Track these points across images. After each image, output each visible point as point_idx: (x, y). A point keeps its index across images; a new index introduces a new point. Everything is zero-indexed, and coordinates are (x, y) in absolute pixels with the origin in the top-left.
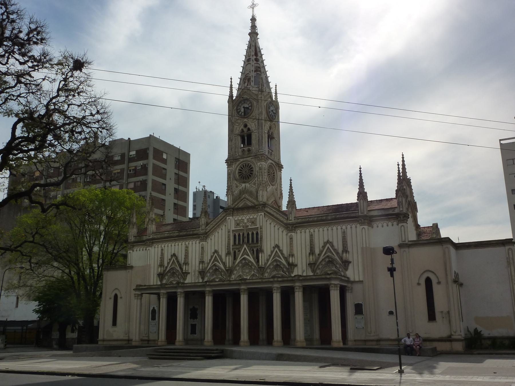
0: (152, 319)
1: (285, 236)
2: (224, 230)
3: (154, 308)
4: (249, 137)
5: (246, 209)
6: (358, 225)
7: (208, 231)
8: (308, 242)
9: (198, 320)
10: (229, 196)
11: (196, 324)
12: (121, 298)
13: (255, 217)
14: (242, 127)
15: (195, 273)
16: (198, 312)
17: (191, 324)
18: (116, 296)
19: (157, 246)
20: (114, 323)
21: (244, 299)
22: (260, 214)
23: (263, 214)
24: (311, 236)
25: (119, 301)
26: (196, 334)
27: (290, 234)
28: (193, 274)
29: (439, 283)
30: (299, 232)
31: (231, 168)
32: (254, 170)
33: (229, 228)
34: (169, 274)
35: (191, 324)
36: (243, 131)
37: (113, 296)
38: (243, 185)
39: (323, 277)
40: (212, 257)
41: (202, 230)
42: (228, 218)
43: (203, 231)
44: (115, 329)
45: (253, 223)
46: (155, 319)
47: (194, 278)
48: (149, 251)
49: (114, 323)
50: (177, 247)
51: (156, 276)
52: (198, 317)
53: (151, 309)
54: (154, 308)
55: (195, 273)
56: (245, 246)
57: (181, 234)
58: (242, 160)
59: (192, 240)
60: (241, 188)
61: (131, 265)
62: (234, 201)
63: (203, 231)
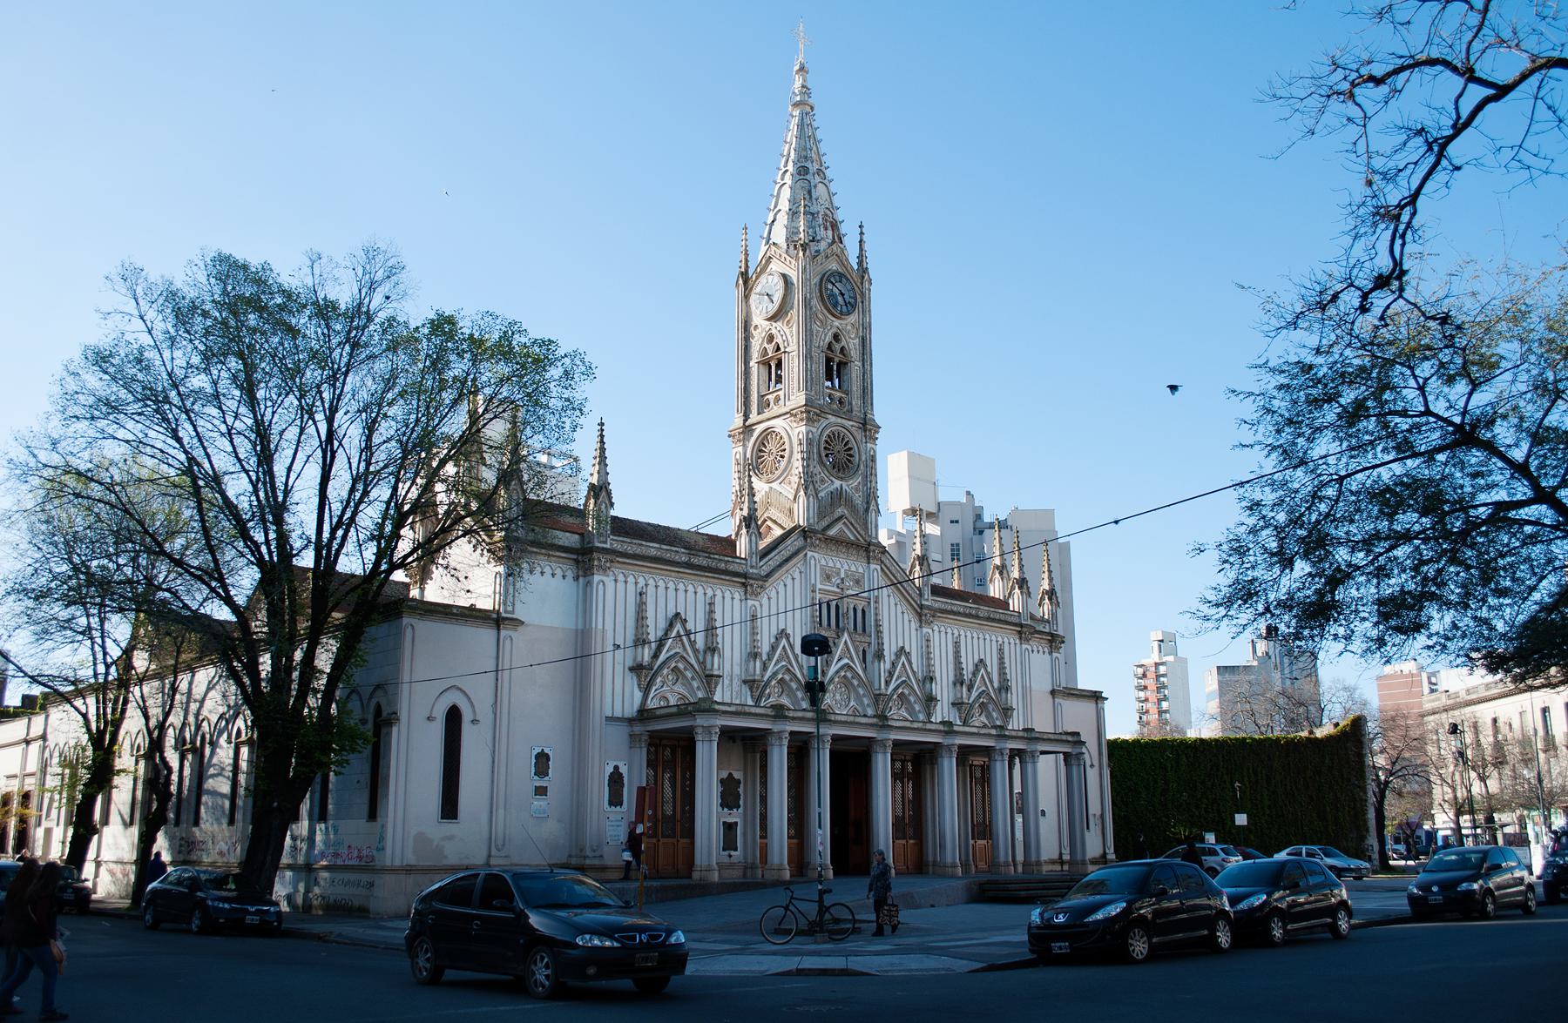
0: (611, 803)
1: (914, 632)
2: (797, 582)
3: (616, 768)
4: (842, 365)
5: (839, 543)
6: (1018, 641)
7: (763, 573)
8: (951, 658)
9: (741, 810)
10: (811, 499)
11: (736, 823)
12: (474, 721)
13: (861, 570)
14: (829, 338)
15: (731, 680)
16: (741, 790)
17: (724, 823)
18: (454, 716)
19: (621, 578)
20: (450, 807)
21: (882, 767)
22: (873, 566)
23: (878, 567)
24: (957, 644)
25: (467, 730)
26: (736, 850)
27: (925, 630)
28: (727, 682)
29: (1092, 766)
30: (936, 628)
31: (814, 430)
32: (857, 456)
33: (813, 582)
34: (665, 671)
35: (724, 823)
36: (830, 347)
37: (440, 713)
38: (837, 483)
39: (1064, 737)
40: (773, 648)
41: (752, 567)
42: (809, 554)
43: (755, 571)
44: (449, 827)
45: (857, 582)
46: (621, 805)
47: (729, 693)
48: (601, 586)
49: (450, 807)
50: (681, 594)
51: (619, 668)
52: (741, 802)
53: (610, 769)
54: (616, 768)
55: (731, 680)
56: (846, 635)
57: (695, 560)
58: (832, 419)
59: (723, 588)
60: (832, 488)
61: (514, 616)
62: (821, 515)
63: (755, 571)
